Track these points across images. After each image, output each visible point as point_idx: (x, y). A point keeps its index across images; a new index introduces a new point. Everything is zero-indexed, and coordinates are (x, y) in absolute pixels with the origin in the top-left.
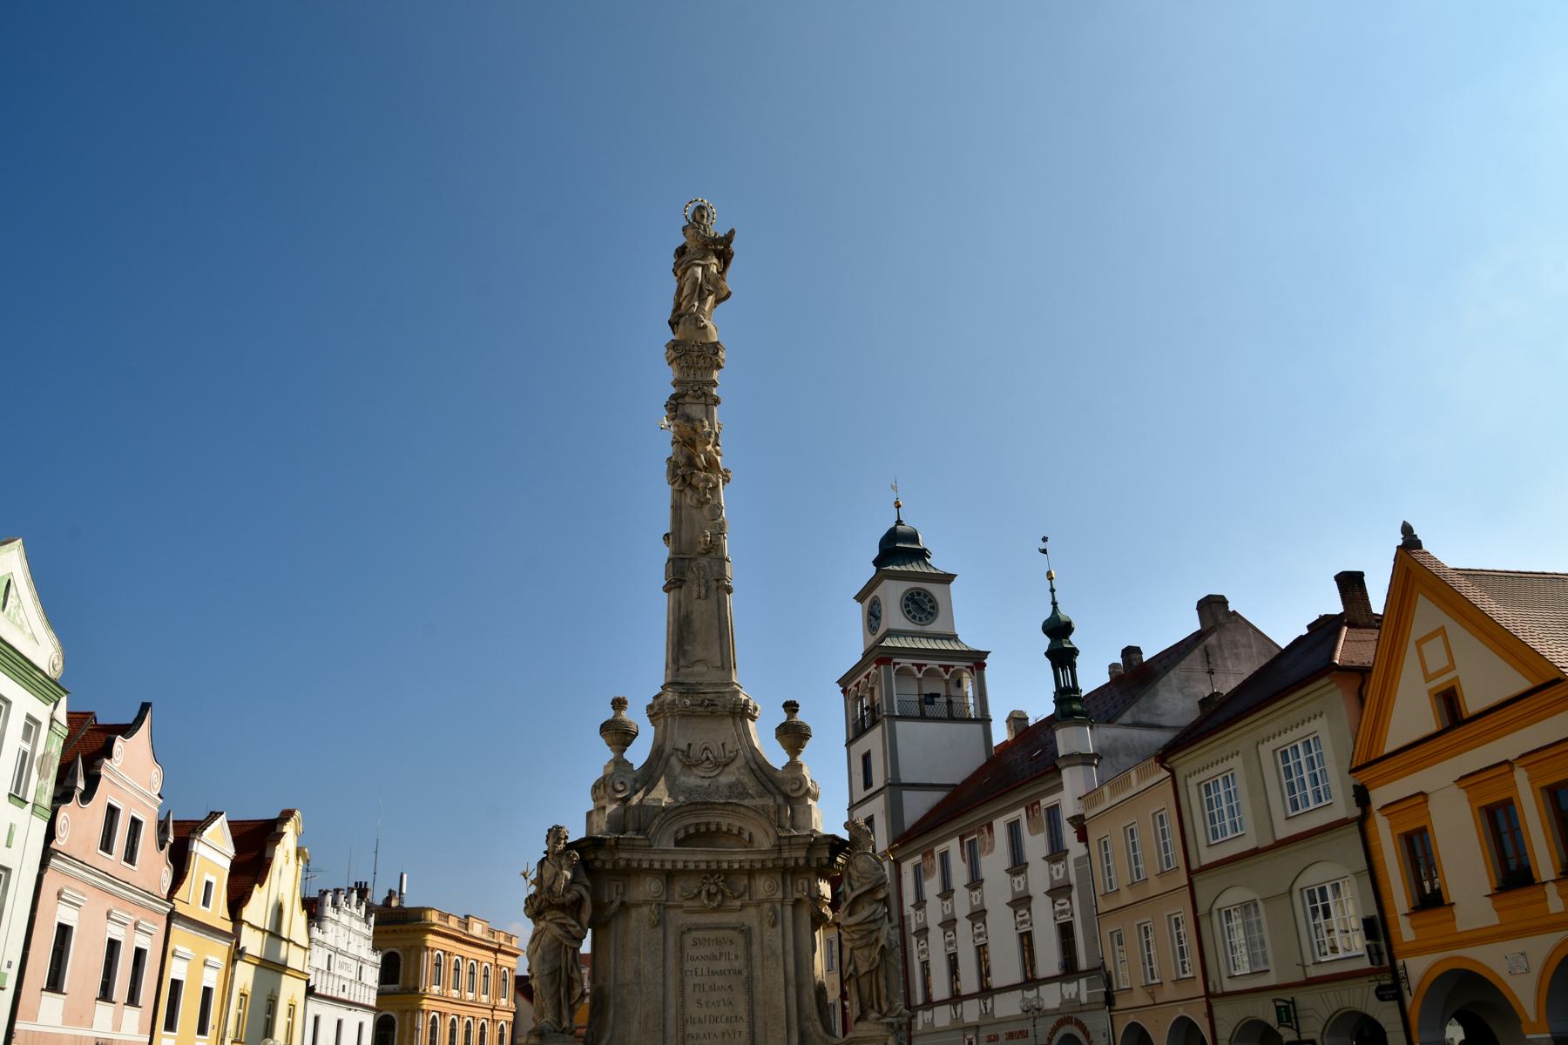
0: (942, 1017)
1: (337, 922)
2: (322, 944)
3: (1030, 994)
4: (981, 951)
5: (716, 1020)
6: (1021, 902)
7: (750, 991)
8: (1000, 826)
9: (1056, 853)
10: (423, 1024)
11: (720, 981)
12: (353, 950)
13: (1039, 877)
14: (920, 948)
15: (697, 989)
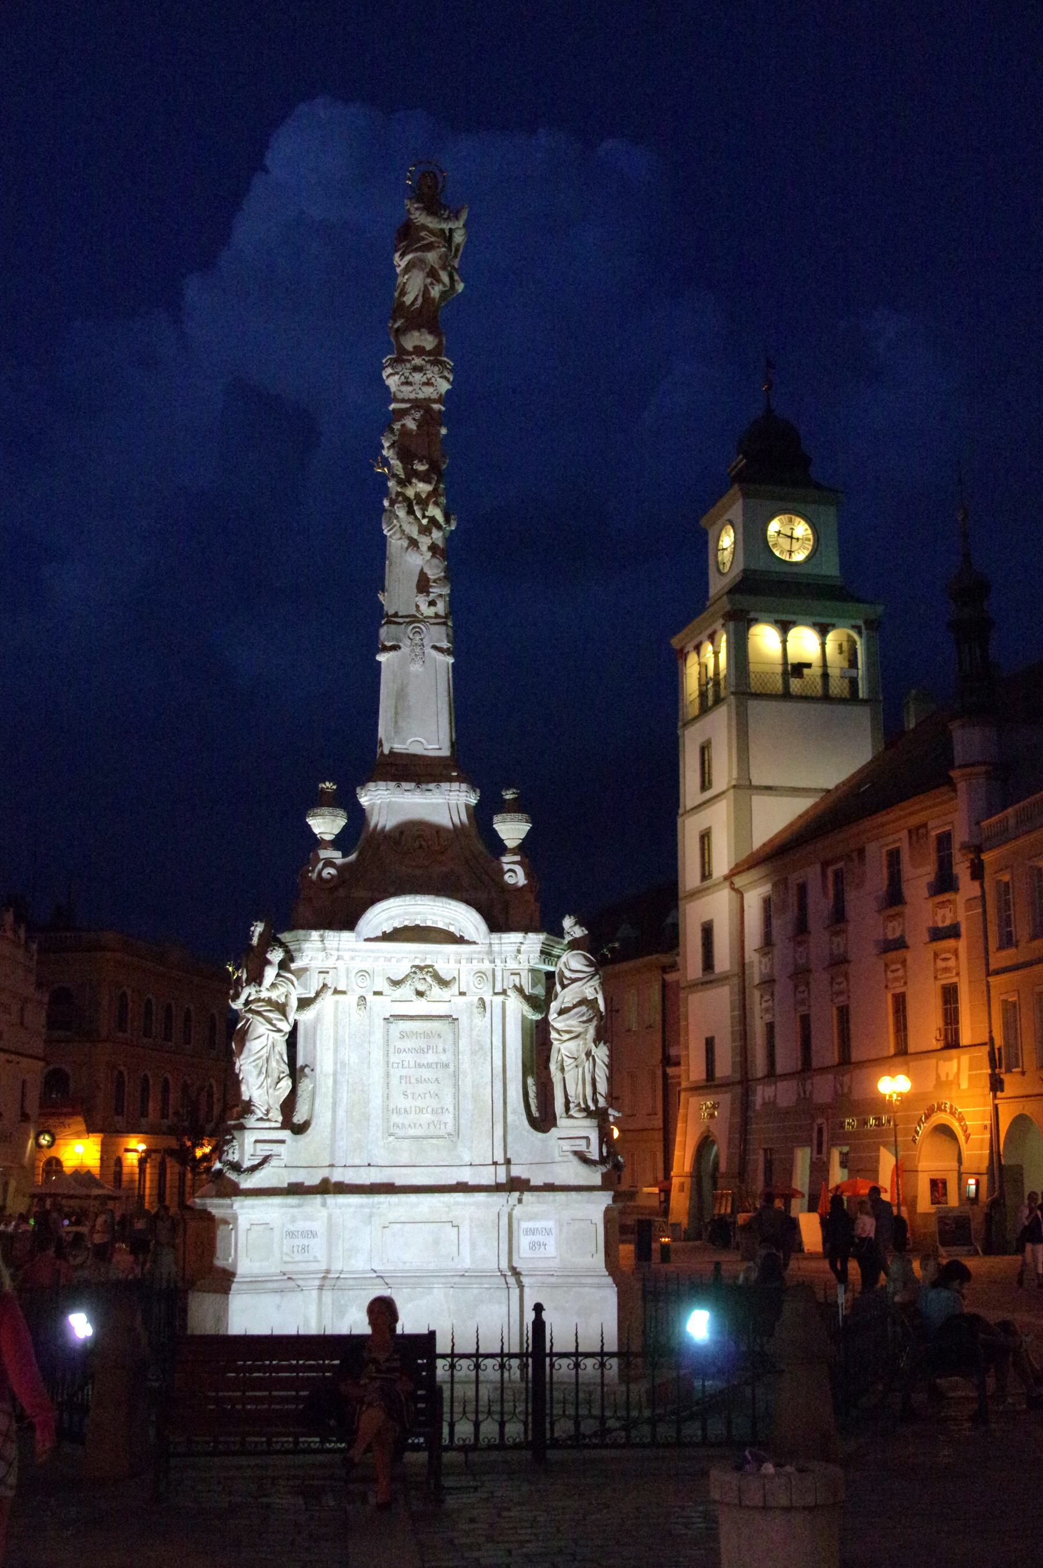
5: (421, 1110)
7: (456, 1086)
11: (426, 1074)
14: (764, 1005)
15: (403, 1081)
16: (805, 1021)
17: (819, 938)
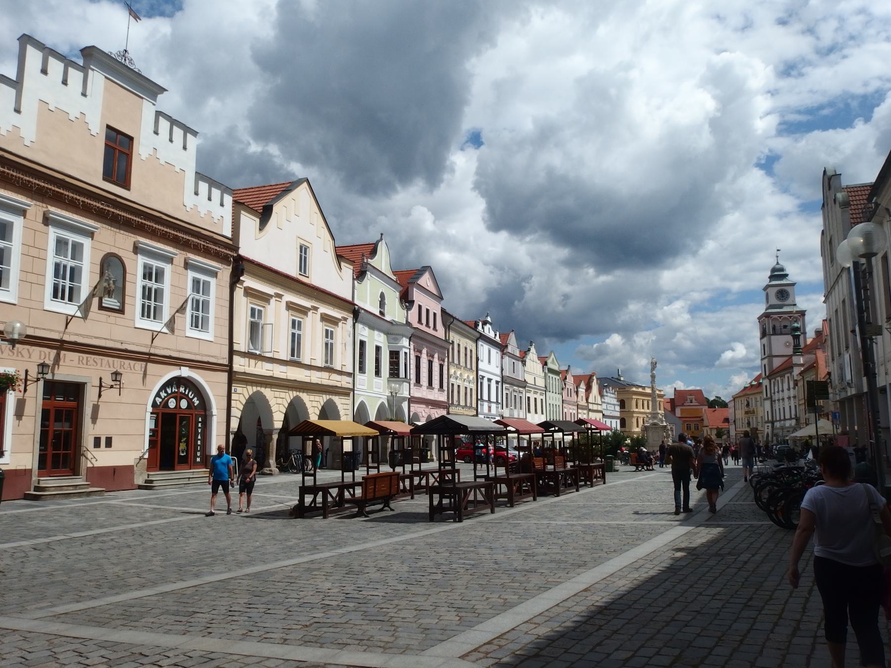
0: (777, 425)
1: (607, 396)
2: (604, 402)
3: (790, 421)
4: (784, 408)
6: (789, 398)
8: (786, 376)
9: (794, 388)
10: (634, 421)
12: (612, 402)
13: (792, 393)
16: (780, 409)
17: (780, 392)
